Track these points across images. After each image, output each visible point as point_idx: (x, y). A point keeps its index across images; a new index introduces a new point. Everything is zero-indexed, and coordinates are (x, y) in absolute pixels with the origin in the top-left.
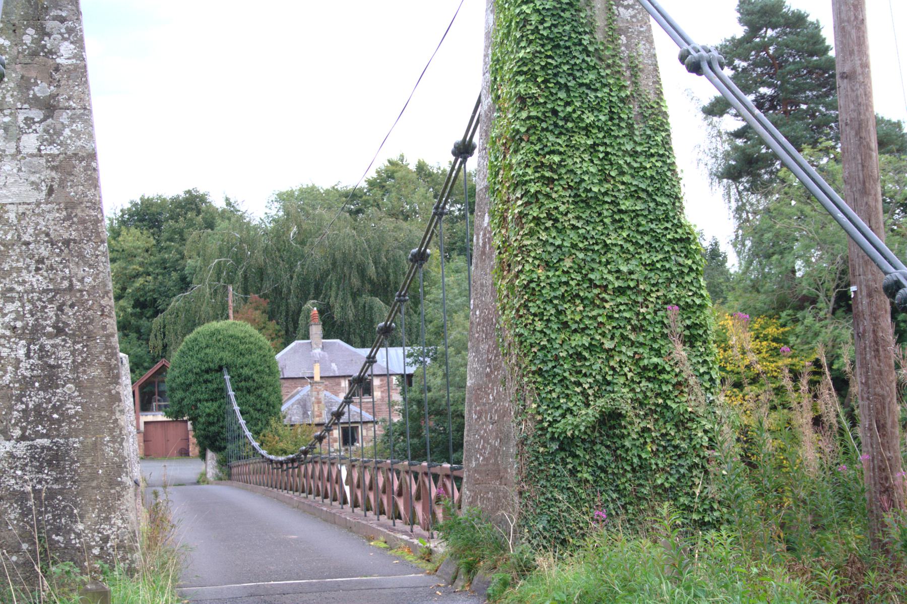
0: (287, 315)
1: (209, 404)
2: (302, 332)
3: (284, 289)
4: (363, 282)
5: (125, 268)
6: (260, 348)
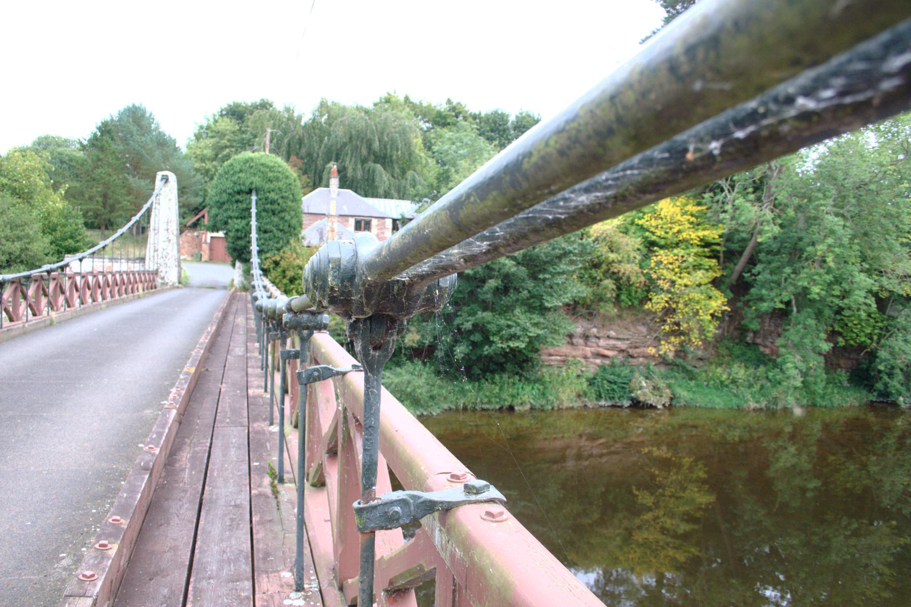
0: (315, 173)
1: (239, 221)
2: (324, 182)
3: (315, 155)
4: (369, 153)
5: (218, 142)
6: (287, 177)
